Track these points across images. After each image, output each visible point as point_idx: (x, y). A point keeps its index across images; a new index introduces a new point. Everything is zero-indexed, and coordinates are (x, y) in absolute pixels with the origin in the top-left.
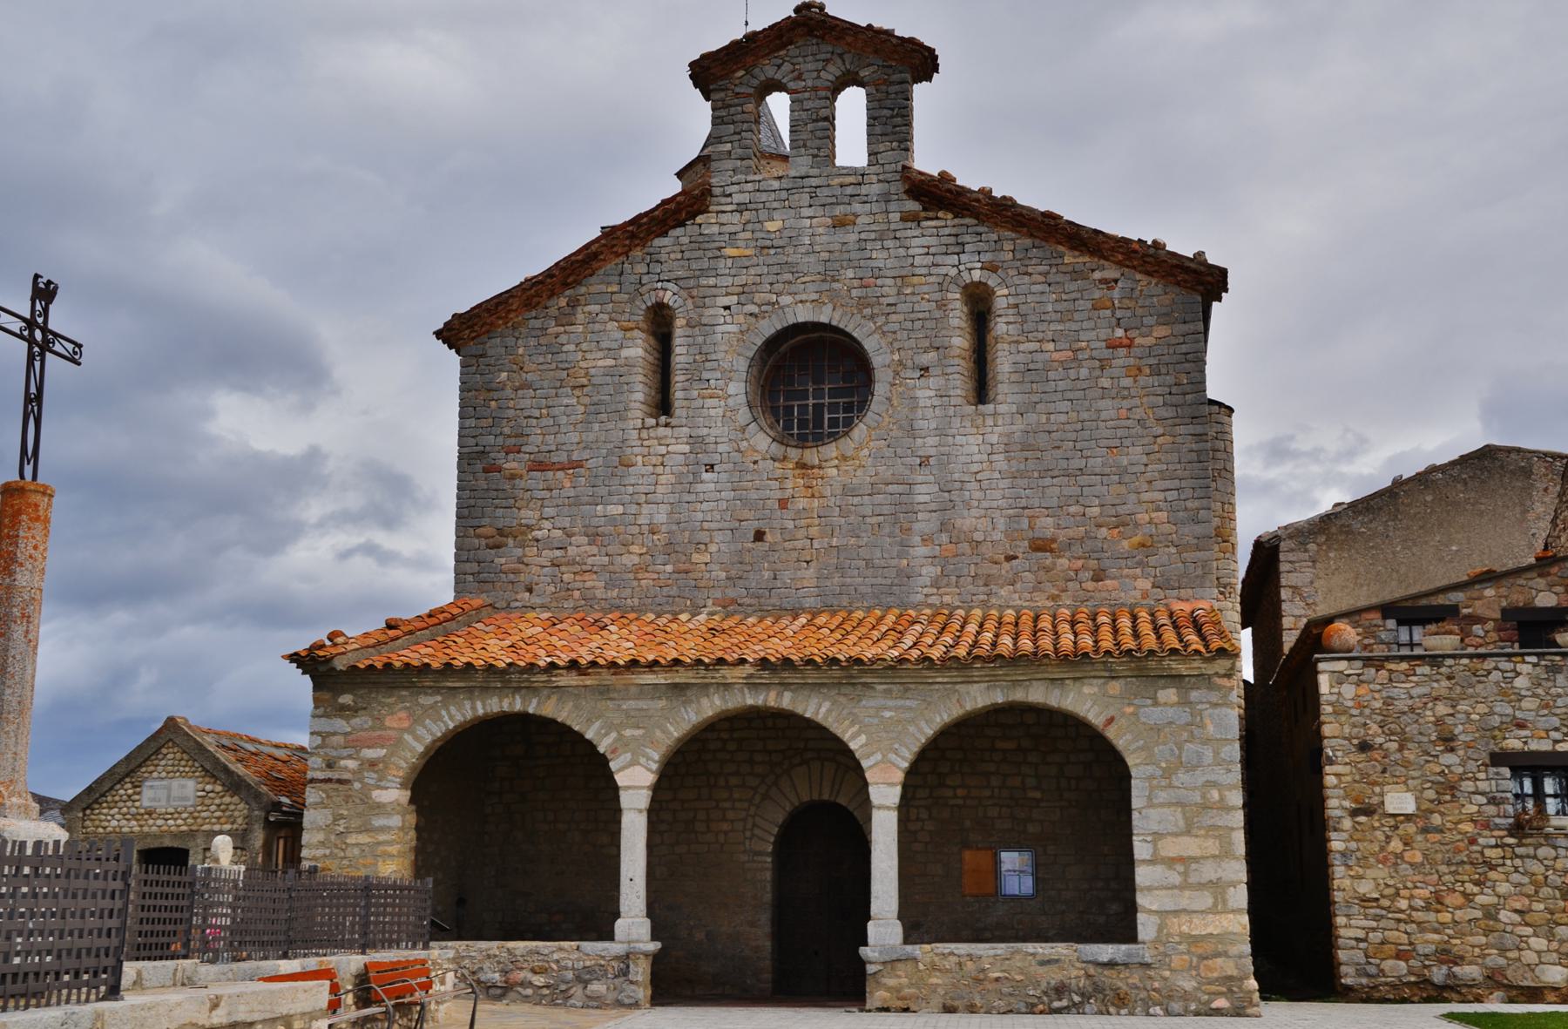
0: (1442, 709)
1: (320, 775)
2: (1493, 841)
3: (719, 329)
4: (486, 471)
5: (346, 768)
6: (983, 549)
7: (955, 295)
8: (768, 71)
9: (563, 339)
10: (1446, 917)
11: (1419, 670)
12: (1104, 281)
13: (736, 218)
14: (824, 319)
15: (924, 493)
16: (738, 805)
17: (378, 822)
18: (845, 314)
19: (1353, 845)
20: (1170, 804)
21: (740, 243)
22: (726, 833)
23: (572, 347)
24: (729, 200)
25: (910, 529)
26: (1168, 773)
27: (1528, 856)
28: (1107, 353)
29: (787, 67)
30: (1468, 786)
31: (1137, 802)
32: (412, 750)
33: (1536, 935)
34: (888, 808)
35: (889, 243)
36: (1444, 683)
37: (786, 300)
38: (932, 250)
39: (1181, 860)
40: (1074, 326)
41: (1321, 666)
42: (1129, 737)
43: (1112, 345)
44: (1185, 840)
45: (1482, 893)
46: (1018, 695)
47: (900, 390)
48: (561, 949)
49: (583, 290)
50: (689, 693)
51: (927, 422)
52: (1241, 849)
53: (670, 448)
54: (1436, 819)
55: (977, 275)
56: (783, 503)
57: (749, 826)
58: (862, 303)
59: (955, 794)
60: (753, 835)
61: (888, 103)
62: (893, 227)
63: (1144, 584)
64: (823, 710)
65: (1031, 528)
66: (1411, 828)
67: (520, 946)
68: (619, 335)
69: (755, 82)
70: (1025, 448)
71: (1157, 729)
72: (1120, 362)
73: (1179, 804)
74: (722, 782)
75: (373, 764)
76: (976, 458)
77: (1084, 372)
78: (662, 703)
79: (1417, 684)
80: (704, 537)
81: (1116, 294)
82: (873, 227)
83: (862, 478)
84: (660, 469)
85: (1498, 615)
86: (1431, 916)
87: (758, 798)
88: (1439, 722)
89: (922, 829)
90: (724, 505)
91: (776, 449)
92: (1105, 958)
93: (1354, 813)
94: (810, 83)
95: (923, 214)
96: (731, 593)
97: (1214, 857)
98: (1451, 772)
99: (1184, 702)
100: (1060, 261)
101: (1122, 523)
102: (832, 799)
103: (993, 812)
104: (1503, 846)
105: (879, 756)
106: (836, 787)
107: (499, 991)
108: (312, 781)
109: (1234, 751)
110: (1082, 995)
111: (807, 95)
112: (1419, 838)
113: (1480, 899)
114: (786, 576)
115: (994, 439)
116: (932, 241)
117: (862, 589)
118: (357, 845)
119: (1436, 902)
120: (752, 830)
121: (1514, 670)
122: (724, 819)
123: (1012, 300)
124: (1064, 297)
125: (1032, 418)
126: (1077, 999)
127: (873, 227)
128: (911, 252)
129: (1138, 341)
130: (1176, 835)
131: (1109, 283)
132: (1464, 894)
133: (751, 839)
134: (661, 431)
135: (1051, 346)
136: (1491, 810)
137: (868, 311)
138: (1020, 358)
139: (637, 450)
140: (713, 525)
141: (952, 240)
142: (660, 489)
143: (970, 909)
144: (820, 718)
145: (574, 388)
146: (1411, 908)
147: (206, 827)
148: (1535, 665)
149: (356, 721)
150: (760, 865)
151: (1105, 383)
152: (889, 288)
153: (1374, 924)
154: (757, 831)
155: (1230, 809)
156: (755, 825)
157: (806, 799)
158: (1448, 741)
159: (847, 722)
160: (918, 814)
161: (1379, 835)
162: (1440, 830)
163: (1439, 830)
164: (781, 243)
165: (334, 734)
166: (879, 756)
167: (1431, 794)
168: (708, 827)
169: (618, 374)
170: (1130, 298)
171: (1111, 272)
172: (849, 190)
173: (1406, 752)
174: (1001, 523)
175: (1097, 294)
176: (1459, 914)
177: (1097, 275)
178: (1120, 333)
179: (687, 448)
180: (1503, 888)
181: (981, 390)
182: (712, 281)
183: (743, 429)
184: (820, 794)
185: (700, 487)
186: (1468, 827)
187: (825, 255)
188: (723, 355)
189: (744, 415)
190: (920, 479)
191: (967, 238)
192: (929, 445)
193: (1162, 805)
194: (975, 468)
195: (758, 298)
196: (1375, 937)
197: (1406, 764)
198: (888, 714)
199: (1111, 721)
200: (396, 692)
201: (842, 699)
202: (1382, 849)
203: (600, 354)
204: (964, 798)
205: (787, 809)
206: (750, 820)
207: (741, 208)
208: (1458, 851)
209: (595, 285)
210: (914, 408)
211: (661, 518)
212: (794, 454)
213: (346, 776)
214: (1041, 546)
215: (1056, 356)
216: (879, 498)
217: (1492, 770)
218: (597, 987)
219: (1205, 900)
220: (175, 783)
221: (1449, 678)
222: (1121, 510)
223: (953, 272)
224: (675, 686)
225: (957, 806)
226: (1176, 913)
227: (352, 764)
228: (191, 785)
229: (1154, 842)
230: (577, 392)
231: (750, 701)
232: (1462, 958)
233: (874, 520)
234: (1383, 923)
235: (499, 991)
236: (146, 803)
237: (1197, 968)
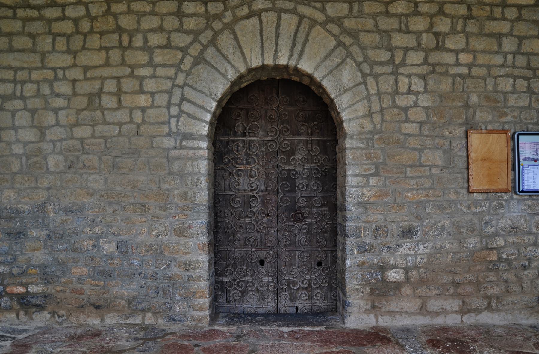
16: (160, 71)
22: (143, 110)
57: (176, 99)
59: (457, 60)
60: (181, 112)
74: (138, 41)
87: (188, 62)
89: (416, 105)
102: (292, 63)
103: (506, 85)
106: (298, 47)
120: (180, 105)
122: (141, 91)
133: (178, 117)
143: (478, 210)
150: (191, 152)
154: (186, 107)
156: (183, 99)
157: (256, 63)
160: (410, 84)
168: (120, 102)
184: (276, 57)
204: (470, 66)
205: (229, 77)
206: (177, 93)
225: (459, 75)
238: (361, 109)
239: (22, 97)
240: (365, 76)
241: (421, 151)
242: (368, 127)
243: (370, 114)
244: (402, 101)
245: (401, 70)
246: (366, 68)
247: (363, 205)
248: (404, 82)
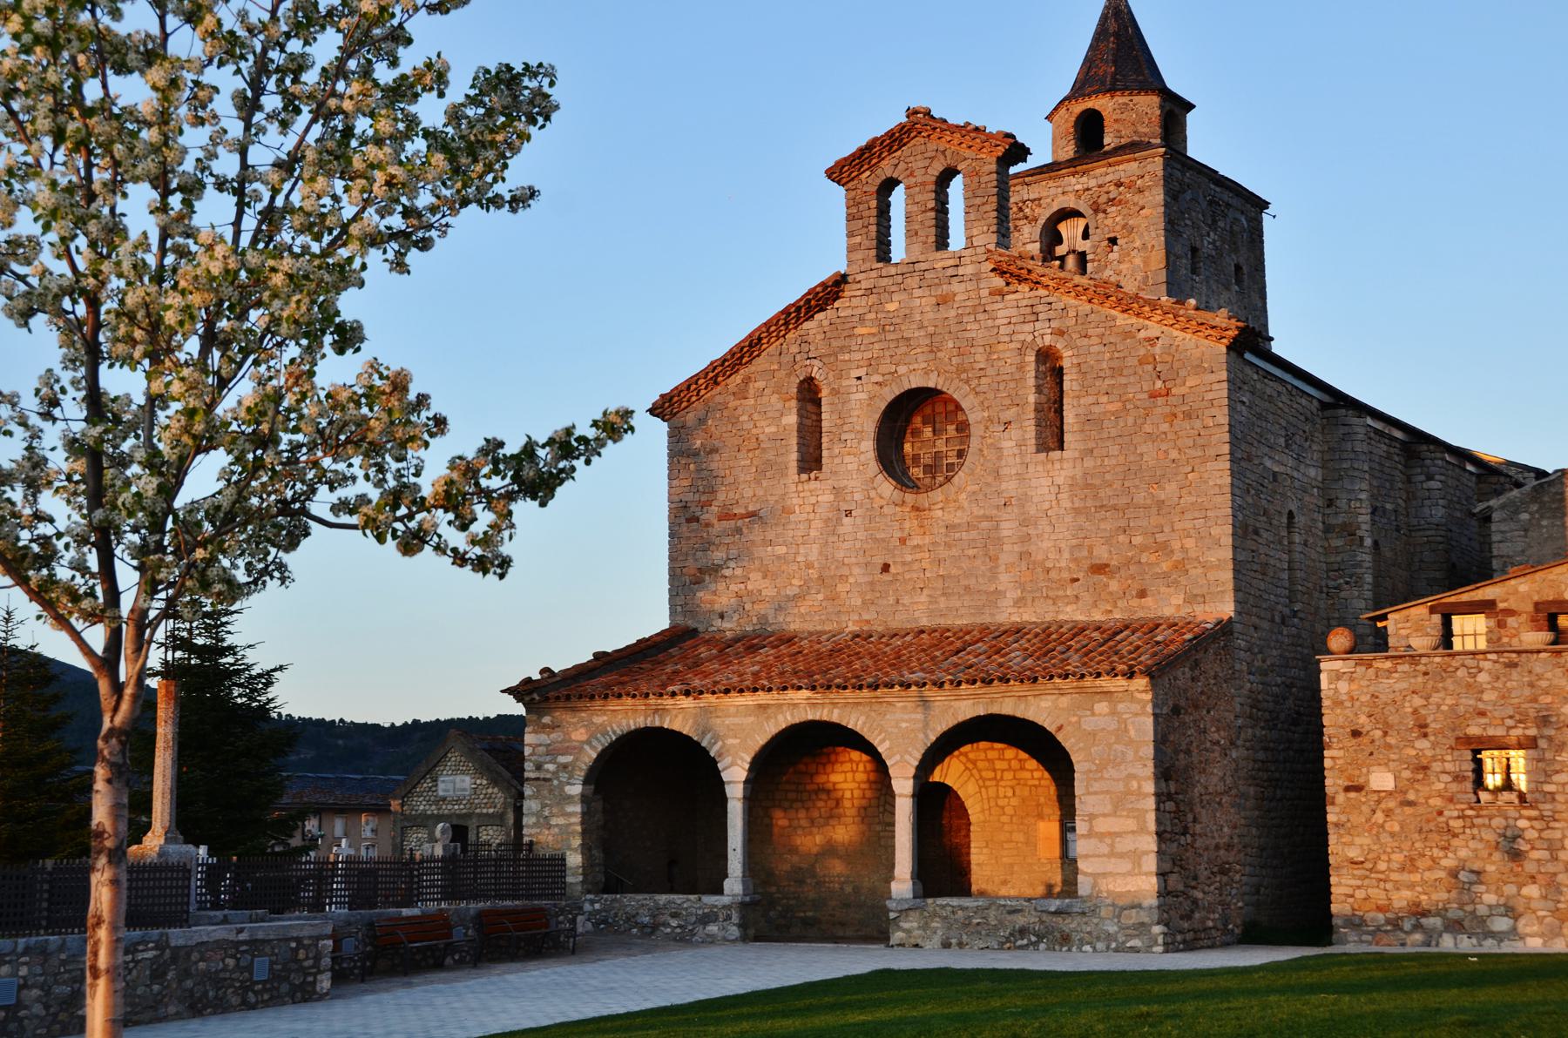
0: (1418, 701)
1: (532, 775)
2: (1456, 814)
3: (853, 397)
4: (689, 521)
5: (547, 771)
6: (1053, 574)
7: (1031, 358)
8: (886, 169)
9: (740, 411)
10: (1416, 877)
11: (1400, 668)
12: (1149, 340)
13: (864, 301)
14: (931, 385)
15: (1008, 529)
17: (569, 809)
18: (946, 379)
19: (1343, 818)
20: (1102, 792)
21: (868, 323)
23: (745, 418)
24: (858, 286)
25: (998, 559)
26: (1101, 768)
27: (1484, 825)
28: (1148, 403)
29: (902, 166)
30: (1436, 766)
31: (1077, 792)
32: (589, 756)
33: (1487, 892)
34: (906, 796)
35: (981, 317)
36: (1420, 679)
37: (902, 370)
38: (1013, 320)
39: (1110, 834)
40: (1123, 380)
41: (1323, 666)
42: (1073, 740)
43: (1153, 395)
44: (1111, 820)
45: (1446, 857)
46: (995, 709)
47: (989, 441)
48: (688, 900)
49: (752, 368)
50: (769, 711)
51: (1010, 467)
52: (1152, 826)
53: (820, 498)
54: (1411, 796)
55: (1048, 340)
56: (903, 541)
57: (882, 803)
58: (960, 370)
61: (979, 192)
62: (983, 301)
63: (1178, 599)
64: (860, 722)
65: (1091, 552)
66: (1391, 804)
67: (663, 898)
68: (779, 406)
69: (878, 181)
70: (1088, 486)
71: (1093, 734)
72: (1159, 410)
73: (1107, 792)
75: (565, 767)
76: (1048, 497)
77: (1130, 421)
78: (752, 719)
79: (1398, 680)
80: (845, 571)
81: (1157, 350)
82: (968, 303)
83: (959, 518)
84: (812, 516)
85: (1530, 608)
86: (1405, 877)
88: (1415, 711)
90: (858, 545)
91: (897, 495)
92: (1053, 909)
93: (1347, 789)
94: (919, 180)
95: (1006, 289)
96: (866, 617)
97: (1133, 832)
98: (1424, 755)
99: (1113, 713)
100: (1112, 323)
101: (1163, 548)
104: (1463, 817)
105: (898, 757)
107: (649, 930)
108: (528, 779)
109: (1149, 751)
110: (1037, 936)
111: (917, 189)
112: (1398, 811)
113: (1444, 862)
114: (906, 600)
115: (1060, 480)
116: (1014, 312)
117: (962, 611)
118: (557, 825)
119: (1410, 865)
121: (1478, 667)
123: (1075, 361)
124: (1116, 355)
125: (1089, 463)
126: (1033, 939)
127: (968, 303)
128: (998, 322)
129: (1174, 391)
130: (1104, 815)
131: (1152, 341)
132: (1433, 859)
134: (813, 485)
135: (1104, 399)
136: (1454, 787)
137: (964, 376)
138: (1081, 411)
139: (795, 501)
140: (853, 560)
141: (1028, 310)
142: (813, 533)
144: (858, 729)
145: (749, 451)
146: (1389, 869)
147: (478, 811)
148: (1495, 662)
149: (553, 736)
151: (1148, 428)
152: (980, 358)
153: (1359, 883)
155: (1140, 794)
158: (1422, 728)
159: (876, 732)
161: (1365, 809)
162: (1411, 804)
163: (1411, 804)
164: (898, 321)
165: (540, 745)
166: (898, 757)
167: (1406, 774)
169: (778, 439)
170: (1169, 354)
171: (1153, 329)
172: (951, 272)
173: (1388, 739)
174: (1066, 555)
175: (1142, 352)
176: (1427, 875)
177: (1142, 334)
178: (1159, 384)
179: (832, 497)
180: (1463, 853)
181: (1052, 435)
182: (847, 357)
183: (872, 480)
185: (841, 530)
186: (1436, 802)
187: (931, 329)
188: (855, 419)
189: (873, 466)
190: (1006, 516)
191: (1040, 308)
192: (1010, 487)
193: (1096, 793)
194: (1046, 505)
195: (883, 369)
196: (1360, 894)
197: (1389, 747)
198: (904, 725)
199: (1060, 728)
200: (578, 714)
201: (873, 714)
202: (1368, 820)
203: (768, 422)
204: (1040, 779)
207: (870, 291)
208: (1428, 821)
209: (761, 363)
210: (1000, 458)
211: (814, 553)
212: (910, 498)
213: (548, 776)
214: (1100, 569)
215: (1110, 407)
216: (974, 534)
217: (1456, 753)
218: (713, 928)
219: (1125, 866)
220: (458, 778)
221: (1426, 674)
222: (1160, 538)
223: (1029, 338)
224: (760, 706)
226: (1104, 875)
227: (551, 767)
228: (467, 779)
229: (1090, 821)
230: (750, 455)
231: (810, 717)
232: (1429, 911)
233: (971, 552)
234: (1366, 882)
235: (649, 930)
236: (441, 793)
237: (1119, 916)
238: (978, 807)
239: (802, 801)
240: (980, 787)
241: (1011, 832)
242: (982, 818)
243: (983, 811)
244: (1001, 802)
245: (1001, 783)
246: (981, 782)
247: (978, 864)
248: (1002, 790)
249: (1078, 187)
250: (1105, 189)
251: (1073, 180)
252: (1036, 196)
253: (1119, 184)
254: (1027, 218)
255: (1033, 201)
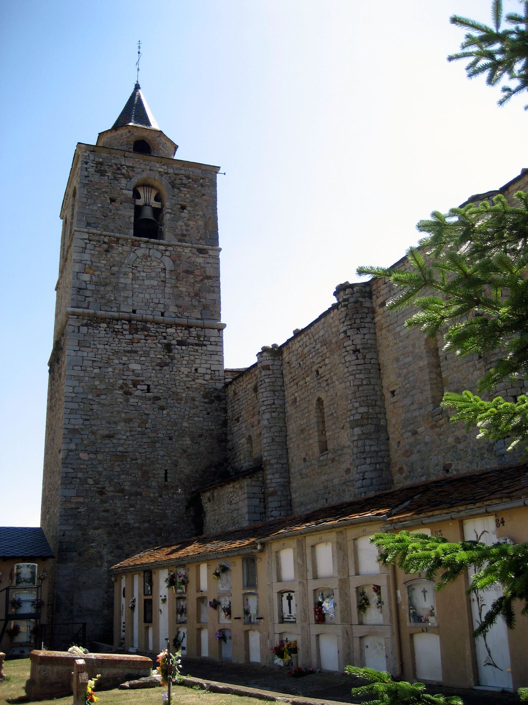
249: (162, 170)
250: (180, 177)
251: (158, 165)
252: (131, 165)
253: (188, 177)
254: (123, 175)
255: (128, 167)
